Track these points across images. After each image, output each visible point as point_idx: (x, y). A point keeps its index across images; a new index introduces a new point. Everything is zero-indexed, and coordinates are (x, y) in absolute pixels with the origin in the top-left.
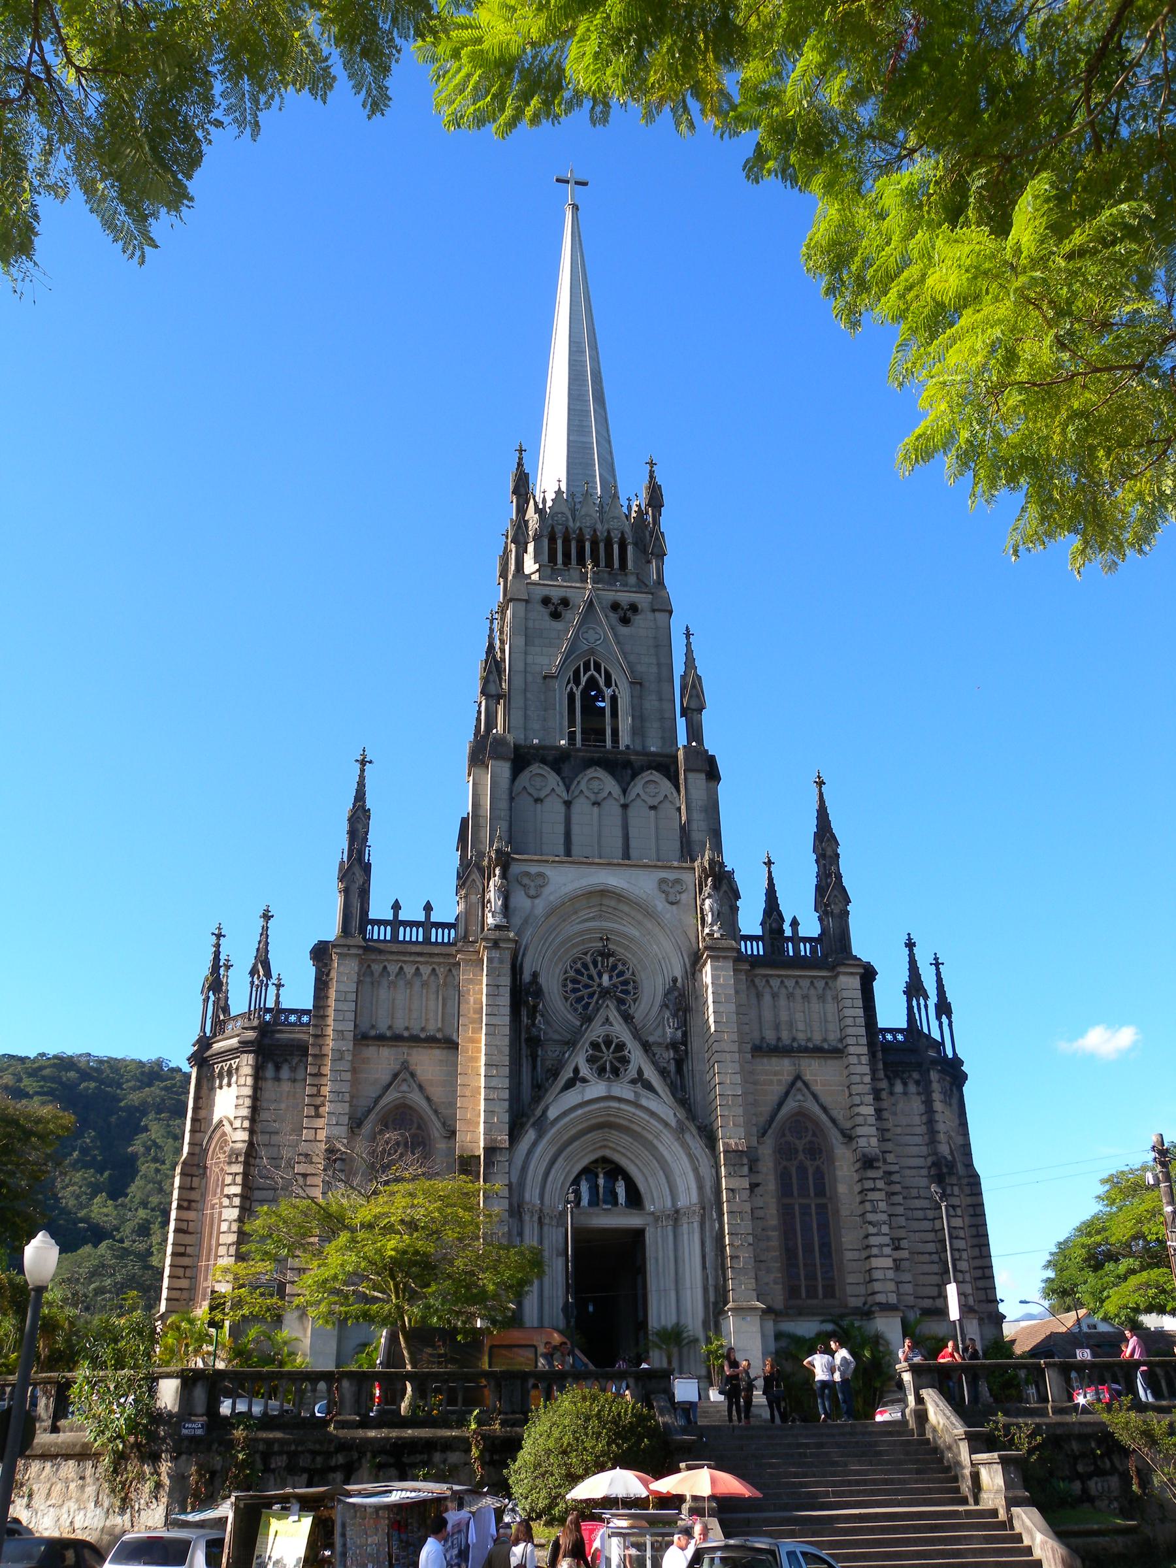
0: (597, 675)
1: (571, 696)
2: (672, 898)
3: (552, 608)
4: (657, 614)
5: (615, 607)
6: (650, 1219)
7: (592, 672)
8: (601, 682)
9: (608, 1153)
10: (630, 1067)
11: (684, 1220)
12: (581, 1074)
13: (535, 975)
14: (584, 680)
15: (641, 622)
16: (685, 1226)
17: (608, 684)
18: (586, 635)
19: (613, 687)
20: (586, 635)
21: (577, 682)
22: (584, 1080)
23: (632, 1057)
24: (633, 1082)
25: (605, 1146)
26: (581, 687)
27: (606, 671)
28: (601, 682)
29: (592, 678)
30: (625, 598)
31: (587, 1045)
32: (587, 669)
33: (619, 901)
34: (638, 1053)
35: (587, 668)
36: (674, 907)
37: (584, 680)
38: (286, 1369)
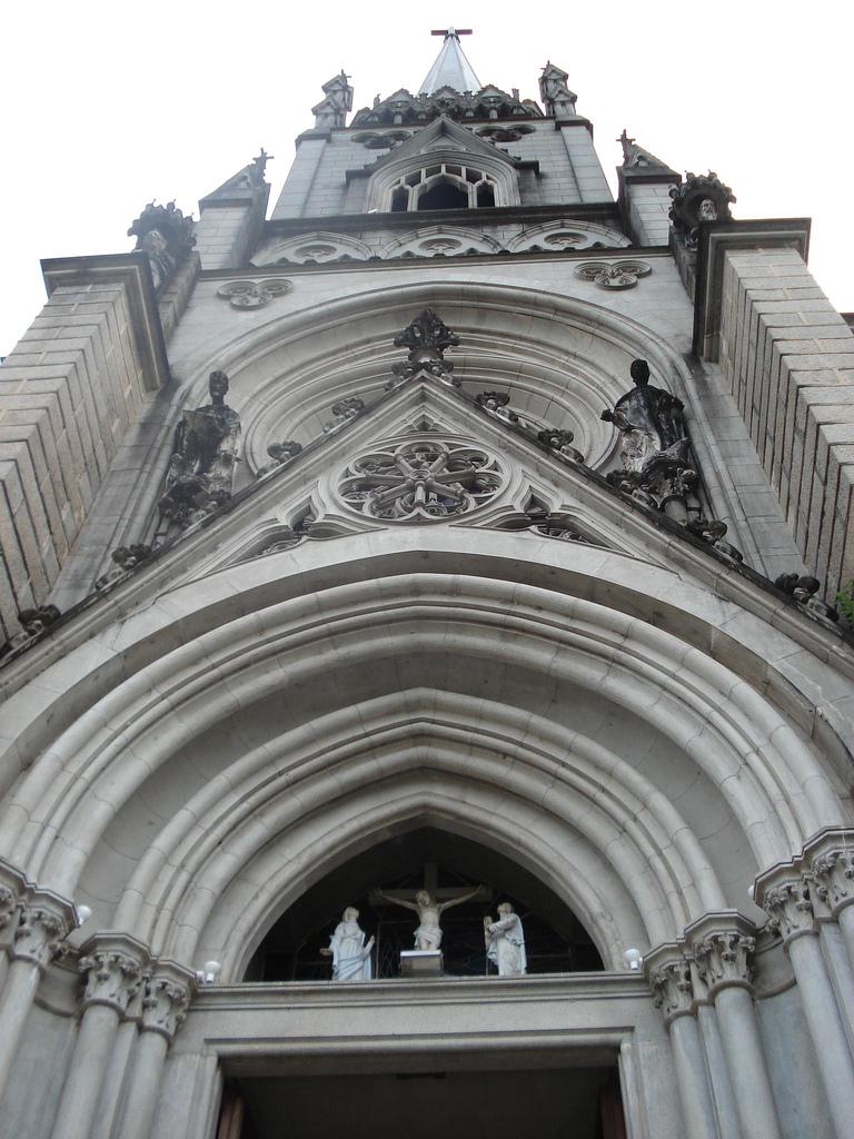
2: (615, 282)
4: (565, 130)
6: (630, 1009)
9: (442, 797)
10: (497, 493)
11: (797, 920)
12: (320, 519)
13: (219, 384)
14: (425, 180)
16: (804, 955)
22: (325, 533)
23: (504, 476)
24: (514, 524)
25: (424, 772)
26: (417, 187)
28: (462, 179)
30: (505, 126)
31: (350, 463)
33: (482, 313)
34: (520, 467)
36: (625, 294)
37: (425, 180)
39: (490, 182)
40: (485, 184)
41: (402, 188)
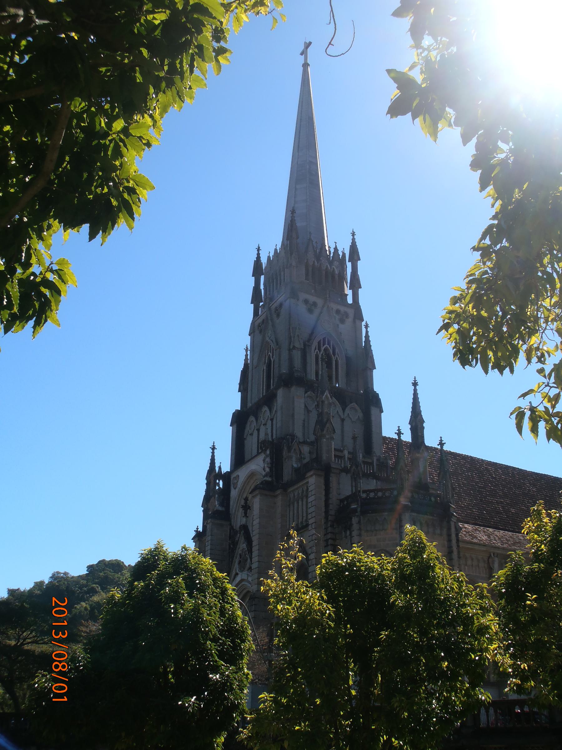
5: (338, 312)
15: (349, 321)
21: (320, 350)
37: (323, 348)
39: (338, 358)
40: (337, 358)
41: (317, 352)
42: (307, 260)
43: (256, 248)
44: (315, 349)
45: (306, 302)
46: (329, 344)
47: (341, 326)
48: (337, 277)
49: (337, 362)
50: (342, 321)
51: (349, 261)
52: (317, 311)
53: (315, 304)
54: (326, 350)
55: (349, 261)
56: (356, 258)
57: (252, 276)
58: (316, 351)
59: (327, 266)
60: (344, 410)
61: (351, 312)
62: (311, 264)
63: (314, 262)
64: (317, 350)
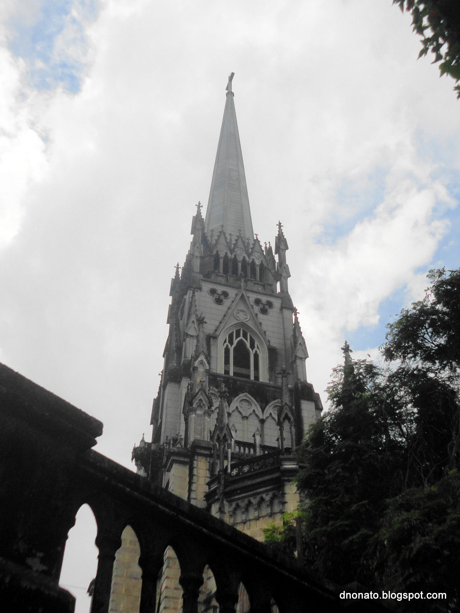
0: (243, 339)
1: (227, 351)
3: (216, 296)
5: (258, 302)
7: (241, 337)
8: (248, 344)
15: (274, 312)
17: (252, 346)
18: (238, 315)
19: (256, 349)
20: (238, 315)
21: (231, 342)
27: (251, 338)
28: (248, 344)
29: (241, 341)
32: (238, 335)
35: (238, 335)
37: (235, 342)
38: (241, 500)
40: (256, 351)
41: (227, 346)
42: (217, 251)
43: (175, 267)
44: (225, 342)
45: (213, 292)
46: (245, 336)
47: (261, 316)
48: (258, 269)
49: (256, 356)
50: (264, 311)
51: (276, 253)
52: (227, 302)
53: (226, 294)
54: (241, 343)
55: (276, 253)
56: (282, 247)
57: (170, 296)
58: (226, 344)
59: (244, 257)
60: (263, 410)
61: (277, 303)
62: (222, 255)
63: (226, 253)
64: (227, 343)
